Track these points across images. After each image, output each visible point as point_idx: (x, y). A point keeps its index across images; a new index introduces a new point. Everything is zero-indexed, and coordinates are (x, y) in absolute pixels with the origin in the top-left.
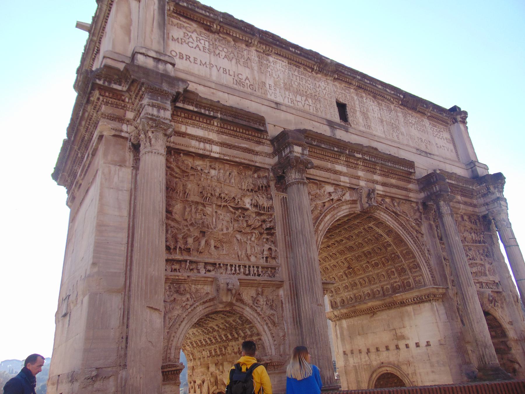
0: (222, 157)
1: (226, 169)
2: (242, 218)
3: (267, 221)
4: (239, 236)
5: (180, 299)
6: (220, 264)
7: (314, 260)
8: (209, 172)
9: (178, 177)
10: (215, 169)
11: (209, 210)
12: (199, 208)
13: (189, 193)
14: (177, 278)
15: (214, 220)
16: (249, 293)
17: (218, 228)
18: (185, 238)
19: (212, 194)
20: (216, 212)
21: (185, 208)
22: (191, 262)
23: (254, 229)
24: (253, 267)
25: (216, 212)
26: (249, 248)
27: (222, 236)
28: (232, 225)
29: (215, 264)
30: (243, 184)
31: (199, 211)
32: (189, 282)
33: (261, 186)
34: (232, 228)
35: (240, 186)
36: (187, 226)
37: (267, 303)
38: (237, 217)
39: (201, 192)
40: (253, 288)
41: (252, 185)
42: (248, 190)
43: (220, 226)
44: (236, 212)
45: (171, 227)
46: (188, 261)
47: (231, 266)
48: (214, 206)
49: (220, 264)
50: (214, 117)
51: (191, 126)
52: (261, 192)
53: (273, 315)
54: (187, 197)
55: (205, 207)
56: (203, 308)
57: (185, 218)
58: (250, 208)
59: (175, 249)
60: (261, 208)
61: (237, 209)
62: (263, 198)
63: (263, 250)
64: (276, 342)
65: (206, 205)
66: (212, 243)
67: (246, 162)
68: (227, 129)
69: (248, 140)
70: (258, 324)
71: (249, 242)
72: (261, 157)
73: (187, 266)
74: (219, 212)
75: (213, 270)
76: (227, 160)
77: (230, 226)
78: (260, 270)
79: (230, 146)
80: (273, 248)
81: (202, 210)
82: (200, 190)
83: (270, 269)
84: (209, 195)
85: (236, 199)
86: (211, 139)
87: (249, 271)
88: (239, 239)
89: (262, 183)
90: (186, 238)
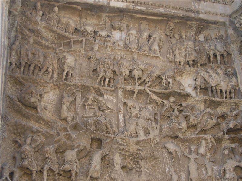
1: (143, 27)
2: (176, 112)
3: (228, 116)
4: (171, 147)
8: (108, 36)
9: (50, 46)
10: (120, 29)
11: (109, 100)
13: (71, 71)
15: (121, 118)
17: (129, 132)
18: (61, 151)
20: (125, 104)
21: (61, 98)
23: (204, 131)
25: (125, 104)
26: (193, 167)
27: (137, 147)
28: (158, 126)
30: (177, 52)
31: (90, 102)
33: (211, 55)
34: (157, 132)
35: (171, 57)
36: (65, 129)
38: (167, 111)
39: (95, 70)
42: (188, 63)
43: (132, 128)
44: (165, 102)
45: (33, 132)
48: (120, 92)
52: (213, 65)
54: (66, 79)
55: (101, 95)
58: (193, 93)
60: (215, 92)
61: (167, 96)
62: (218, 74)
63: (224, 170)
65: (103, 92)
66: (117, 159)
71: (193, 156)
74: (130, 103)
76: (141, 12)
82: (92, 66)
84: (109, 74)
85: (164, 78)
88: (172, 151)
90: (63, 152)
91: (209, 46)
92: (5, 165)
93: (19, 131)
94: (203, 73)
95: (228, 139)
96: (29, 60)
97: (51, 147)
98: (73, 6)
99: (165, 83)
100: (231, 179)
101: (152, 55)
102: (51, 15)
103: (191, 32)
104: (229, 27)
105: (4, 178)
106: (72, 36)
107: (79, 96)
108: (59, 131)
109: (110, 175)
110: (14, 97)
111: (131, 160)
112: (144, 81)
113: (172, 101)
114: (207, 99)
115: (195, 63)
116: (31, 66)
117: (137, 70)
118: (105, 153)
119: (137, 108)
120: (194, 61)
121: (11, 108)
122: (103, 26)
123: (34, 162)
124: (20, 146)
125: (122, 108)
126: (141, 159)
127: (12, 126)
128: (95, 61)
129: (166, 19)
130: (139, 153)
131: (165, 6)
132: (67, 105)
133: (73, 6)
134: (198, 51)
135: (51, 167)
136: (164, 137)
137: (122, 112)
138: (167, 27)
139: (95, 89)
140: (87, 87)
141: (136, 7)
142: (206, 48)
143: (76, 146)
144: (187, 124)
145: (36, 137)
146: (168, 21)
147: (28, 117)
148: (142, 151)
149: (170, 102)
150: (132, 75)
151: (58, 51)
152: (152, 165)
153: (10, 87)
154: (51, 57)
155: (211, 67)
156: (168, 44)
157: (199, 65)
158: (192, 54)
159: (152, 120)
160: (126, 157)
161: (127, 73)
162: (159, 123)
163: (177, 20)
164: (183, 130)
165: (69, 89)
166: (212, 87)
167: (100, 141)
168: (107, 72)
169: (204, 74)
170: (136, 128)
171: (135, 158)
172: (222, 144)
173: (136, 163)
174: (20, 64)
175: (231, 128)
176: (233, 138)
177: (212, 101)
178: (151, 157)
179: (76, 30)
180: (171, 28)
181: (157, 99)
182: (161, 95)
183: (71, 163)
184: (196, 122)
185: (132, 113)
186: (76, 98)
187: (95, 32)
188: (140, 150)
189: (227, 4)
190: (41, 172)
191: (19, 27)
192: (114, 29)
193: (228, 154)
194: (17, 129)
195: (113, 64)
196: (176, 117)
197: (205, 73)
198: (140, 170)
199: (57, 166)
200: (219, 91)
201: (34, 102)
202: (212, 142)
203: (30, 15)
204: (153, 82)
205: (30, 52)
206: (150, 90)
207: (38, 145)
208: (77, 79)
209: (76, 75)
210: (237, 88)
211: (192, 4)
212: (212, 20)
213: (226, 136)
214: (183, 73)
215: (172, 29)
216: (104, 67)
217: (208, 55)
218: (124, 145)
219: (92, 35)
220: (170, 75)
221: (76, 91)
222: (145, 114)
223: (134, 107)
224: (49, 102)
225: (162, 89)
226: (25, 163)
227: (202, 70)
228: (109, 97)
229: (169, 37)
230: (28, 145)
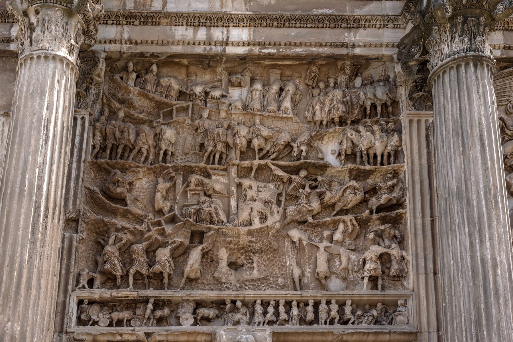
2: (307, 189)
3: (380, 188)
4: (295, 234)
6: (234, 302)
7: (495, 266)
8: (223, 96)
9: (146, 118)
10: (240, 85)
12: (193, 180)
15: (233, 202)
19: (227, 146)
20: (239, 186)
23: (344, 212)
24: (328, 303)
25: (239, 186)
27: (249, 238)
28: (281, 209)
29: (223, 303)
30: (318, 107)
31: (192, 186)
34: (277, 217)
36: (159, 224)
38: (295, 189)
41: (342, 108)
43: (244, 215)
44: (293, 177)
45: (118, 230)
48: (233, 171)
54: (164, 160)
55: (209, 176)
57: (156, 208)
59: (125, 277)
60: (365, 158)
61: (296, 171)
62: (373, 132)
65: (211, 172)
66: (223, 255)
67: (326, 51)
73: (148, 312)
74: (246, 182)
75: (217, 317)
77: (272, 213)
78: (348, 309)
79: (276, 19)
80: (395, 252)
81: (200, 184)
82: (199, 139)
84: (220, 147)
85: (295, 145)
86: (226, 13)
87: (316, 312)
88: (296, 240)
89: (369, 95)
91: (365, 94)
92: (83, 270)
93: (101, 229)
94: (350, 133)
96: (116, 140)
97: (139, 245)
99: (296, 152)
100: (371, 270)
102: (147, 77)
103: (343, 76)
104: (397, 63)
105: (80, 286)
107: (180, 179)
108: (150, 226)
109: (213, 274)
110: (95, 188)
111: (242, 254)
112: (268, 152)
113: (302, 176)
114: (353, 169)
116: (120, 147)
118: (207, 248)
119: (255, 188)
120: (340, 117)
121: (92, 203)
122: (220, 83)
123: (118, 265)
124: (103, 247)
125: (235, 191)
126: (254, 253)
128: (203, 132)
130: (251, 245)
131: (304, 44)
132: (162, 193)
134: (347, 103)
135: (139, 270)
137: (235, 195)
138: (308, 74)
141: (263, 51)
142: (361, 96)
143: (170, 242)
144: (321, 204)
145: (121, 235)
147: (114, 213)
148: (256, 243)
149: (300, 177)
150: (252, 146)
151: (155, 124)
154: (145, 133)
155: (366, 122)
158: (338, 109)
159: (273, 202)
160: (235, 251)
162: (283, 205)
164: (315, 212)
166: (361, 151)
167: (202, 234)
168: (218, 145)
169: (352, 135)
170: (250, 214)
172: (368, 227)
173: (248, 258)
174: (106, 147)
175: (382, 205)
176: (384, 217)
177: (359, 170)
179: (181, 95)
180: (313, 74)
181: (282, 174)
183: (163, 264)
184: (333, 200)
185: (248, 195)
186: (175, 183)
187: (207, 94)
188: (253, 242)
190: (127, 275)
192: (232, 86)
193: (374, 238)
194: (99, 228)
195: (225, 134)
196: (306, 196)
197: (354, 133)
198: (252, 266)
199: (146, 267)
200: (371, 155)
201: (121, 193)
203: (119, 80)
204: (280, 152)
205: (117, 129)
206: (273, 164)
207: (124, 244)
208: (179, 159)
209: (179, 153)
210: (400, 149)
211: (346, 35)
212: (374, 55)
215: (315, 76)
216: (214, 139)
217: (362, 106)
218: (233, 237)
219: (202, 97)
220: (304, 141)
221: (175, 175)
223: (250, 188)
224: (142, 191)
225: (293, 161)
226: (108, 266)
227: (351, 129)
228: (218, 177)
229: (310, 87)
230: (111, 246)
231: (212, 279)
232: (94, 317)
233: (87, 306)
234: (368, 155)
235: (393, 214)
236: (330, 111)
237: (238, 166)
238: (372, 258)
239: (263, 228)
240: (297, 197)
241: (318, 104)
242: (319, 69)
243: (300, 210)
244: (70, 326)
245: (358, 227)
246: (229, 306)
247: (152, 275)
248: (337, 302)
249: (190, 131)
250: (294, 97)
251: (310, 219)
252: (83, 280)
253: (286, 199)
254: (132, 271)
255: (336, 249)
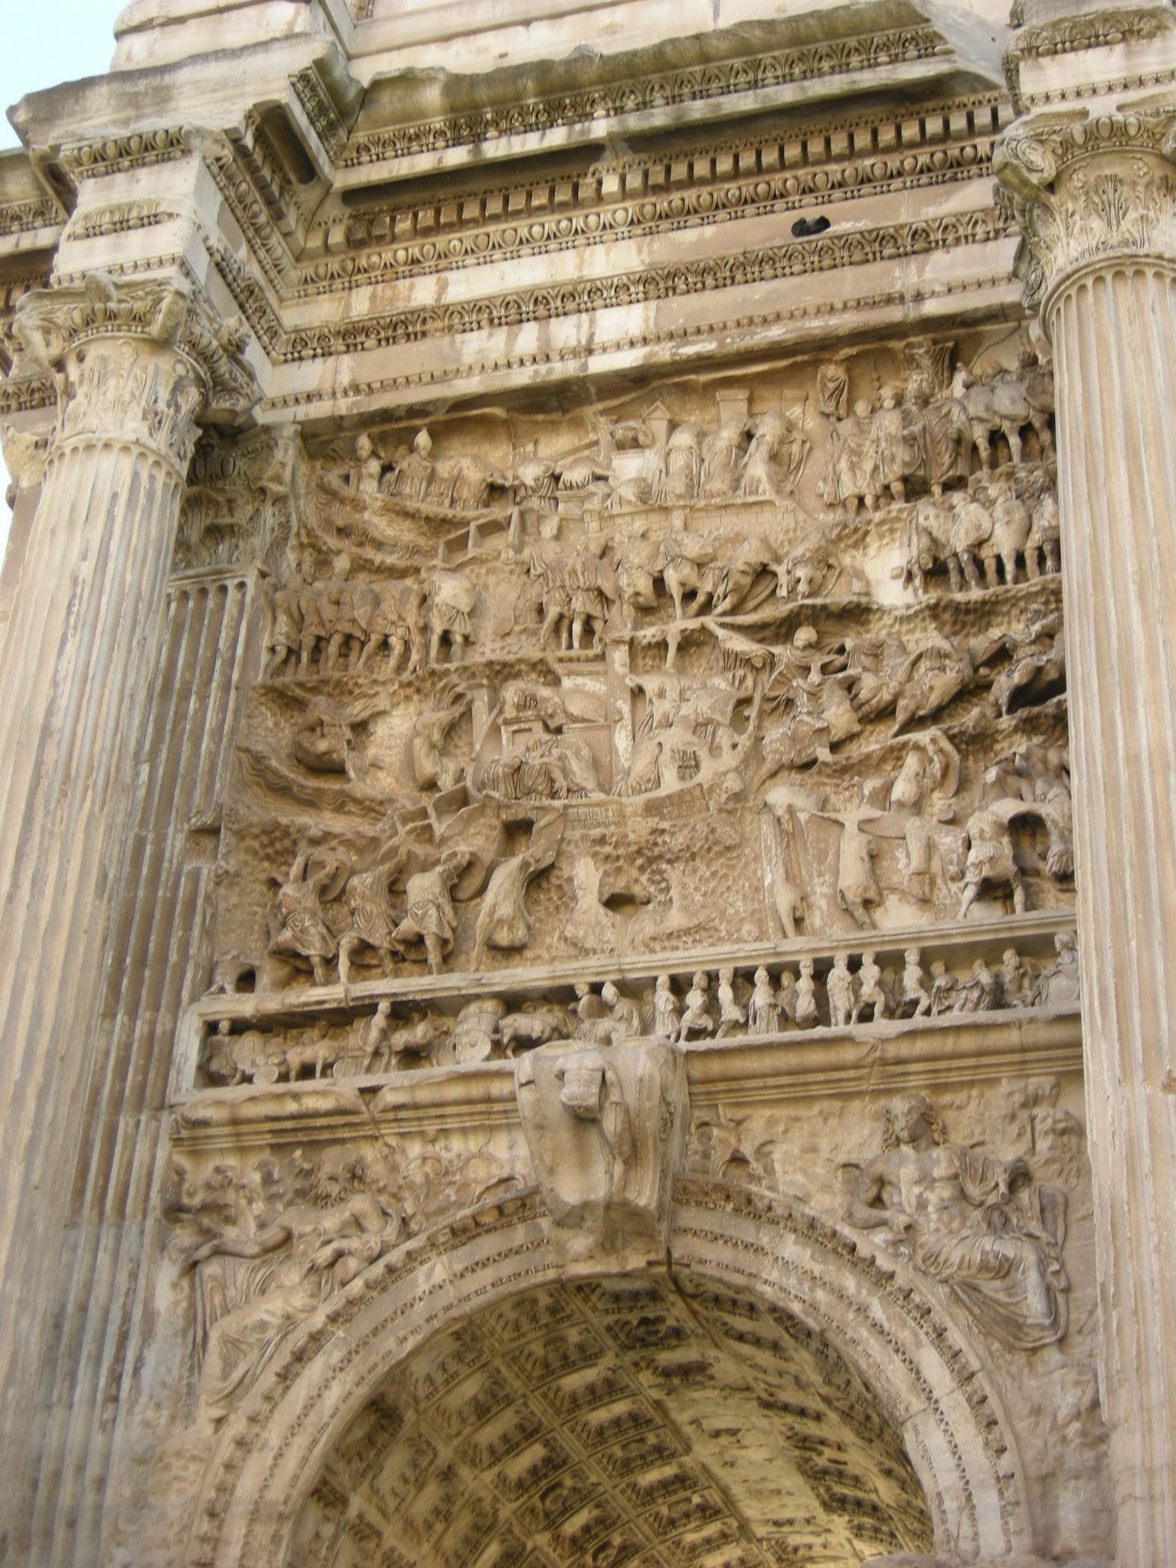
0: (664, 353)
1: (725, 415)
2: (815, 677)
4: (780, 795)
5: (308, 1229)
10: (635, 444)
14: (292, 1107)
16: (824, 1144)
22: (403, 1012)
23: (915, 722)
24: (854, 965)
25: (638, 693)
27: (653, 822)
28: (744, 741)
32: (376, 1122)
34: (729, 759)
37: (963, 1195)
40: (856, 1105)
41: (902, 454)
44: (776, 650)
46: (384, 1006)
47: (679, 986)
48: (619, 656)
49: (596, 989)
50: (591, 151)
51: (471, 260)
53: (1004, 1269)
56: (459, 1267)
59: (330, 962)
60: (970, 570)
61: (783, 630)
64: (1006, 1462)
65: (559, 668)
68: (691, 181)
69: (866, 189)
70: (874, 1345)
72: (962, 251)
76: (703, 363)
78: (912, 974)
81: (528, 702)
82: (533, 593)
83: (1009, 957)
85: (780, 570)
95: (1016, 729)
98: (474, 412)
101: (739, 501)
105: (214, 988)
106: (471, 513)
111: (642, 869)
112: (710, 596)
115: (915, 488)
117: (675, 568)
119: (672, 694)
120: (905, 480)
121: (259, 785)
123: (313, 930)
126: (670, 862)
127: (256, 837)
129: (806, 358)
130: (659, 840)
133: (474, 412)
135: (364, 936)
136: (773, 775)
139: (534, 666)
140: (505, 665)
145: (319, 853)
146: (816, 363)
147: (311, 802)
152: (714, 874)
153: (270, 723)
156: (829, 446)
157: (937, 490)
158: (893, 458)
159: (718, 724)
160: (621, 862)
161: (644, 585)
163: (846, 352)
164: (837, 734)
165: (445, 687)
166: (955, 555)
171: (651, 861)
173: (658, 877)
178: (709, 850)
180: (832, 386)
182: (767, 633)
184: (886, 696)
188: (663, 831)
189: (957, 241)
191: (303, 532)
200: (990, 565)
202: (941, 750)
206: (723, 625)
213: (1005, 717)
214: (866, 533)
215: (839, 390)
216: (563, 587)
217: (959, 441)
221: (469, 688)
222: (700, 705)
223: (661, 694)
226: (287, 935)
228: (580, 680)
231: (562, 946)
232: (245, 1067)
233: (227, 1039)
234: (978, 563)
235: (1050, 706)
236: (876, 468)
237: (632, 643)
238: (982, 831)
239: (690, 791)
240: (790, 703)
241: (844, 457)
242: (848, 371)
243: (794, 733)
244: (178, 1089)
245: (956, 757)
246: (585, 1000)
247: (401, 948)
248: (880, 960)
249: (514, 578)
250: (785, 449)
251: (823, 754)
252: (223, 975)
253: (761, 714)
254: (346, 942)
255: (890, 821)
